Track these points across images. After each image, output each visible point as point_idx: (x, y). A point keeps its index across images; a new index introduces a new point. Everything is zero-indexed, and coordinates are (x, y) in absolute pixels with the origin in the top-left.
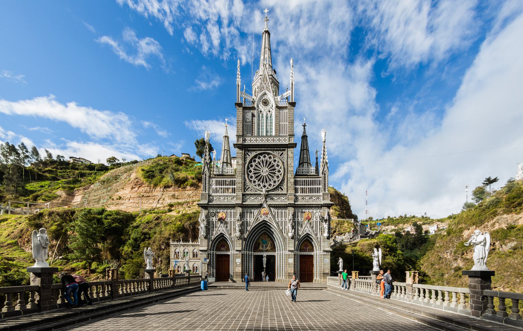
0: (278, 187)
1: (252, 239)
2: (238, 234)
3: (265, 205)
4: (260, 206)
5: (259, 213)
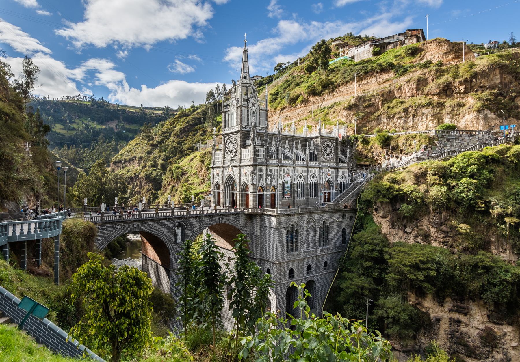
0: (235, 155)
4: (229, 166)
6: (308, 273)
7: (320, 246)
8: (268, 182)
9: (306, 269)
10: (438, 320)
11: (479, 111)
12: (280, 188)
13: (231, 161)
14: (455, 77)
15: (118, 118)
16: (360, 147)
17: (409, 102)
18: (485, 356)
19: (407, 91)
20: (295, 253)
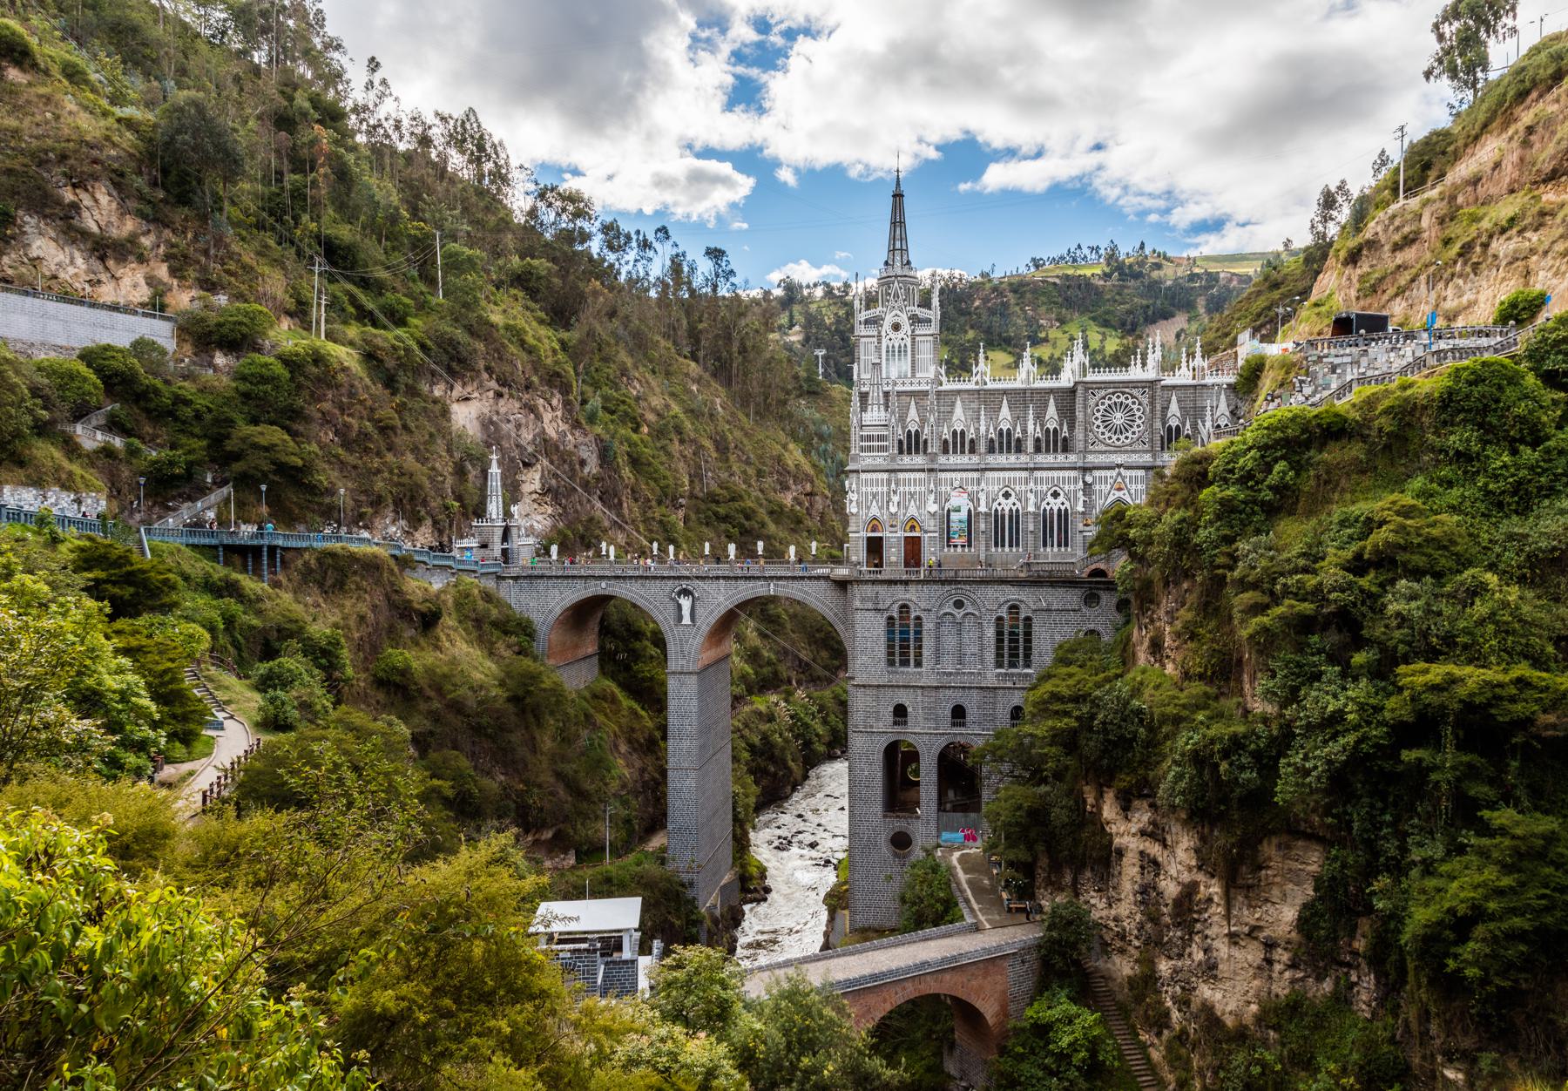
6: (954, 725)
7: (999, 665)
8: (893, 509)
9: (948, 713)
10: (1120, 853)
12: (931, 524)
15: (1189, 306)
18: (1175, 950)
20: (911, 669)
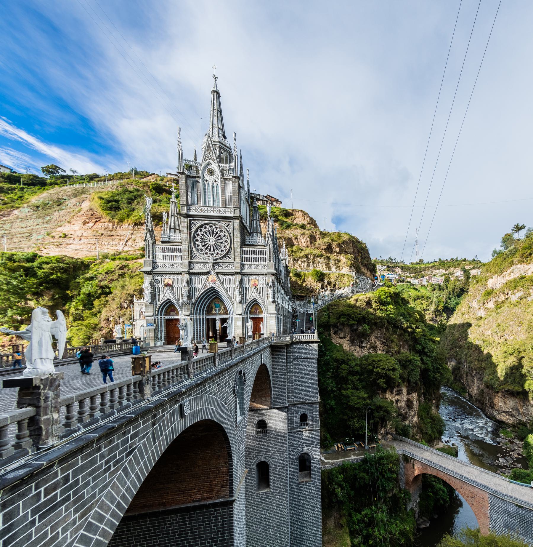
1: (202, 303)
2: (185, 299)
3: (213, 272)
5: (207, 280)
11: (350, 267)
13: (214, 264)
14: (333, 240)
16: (294, 279)
17: (307, 252)
19: (303, 241)
